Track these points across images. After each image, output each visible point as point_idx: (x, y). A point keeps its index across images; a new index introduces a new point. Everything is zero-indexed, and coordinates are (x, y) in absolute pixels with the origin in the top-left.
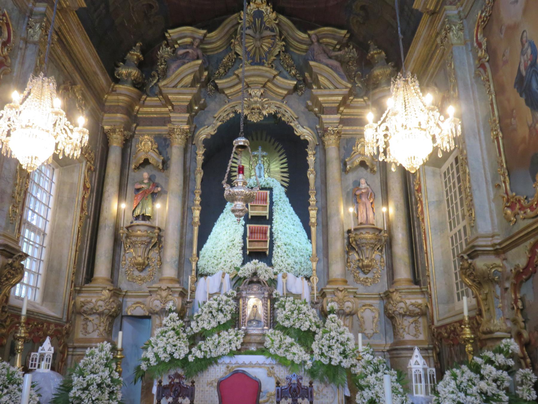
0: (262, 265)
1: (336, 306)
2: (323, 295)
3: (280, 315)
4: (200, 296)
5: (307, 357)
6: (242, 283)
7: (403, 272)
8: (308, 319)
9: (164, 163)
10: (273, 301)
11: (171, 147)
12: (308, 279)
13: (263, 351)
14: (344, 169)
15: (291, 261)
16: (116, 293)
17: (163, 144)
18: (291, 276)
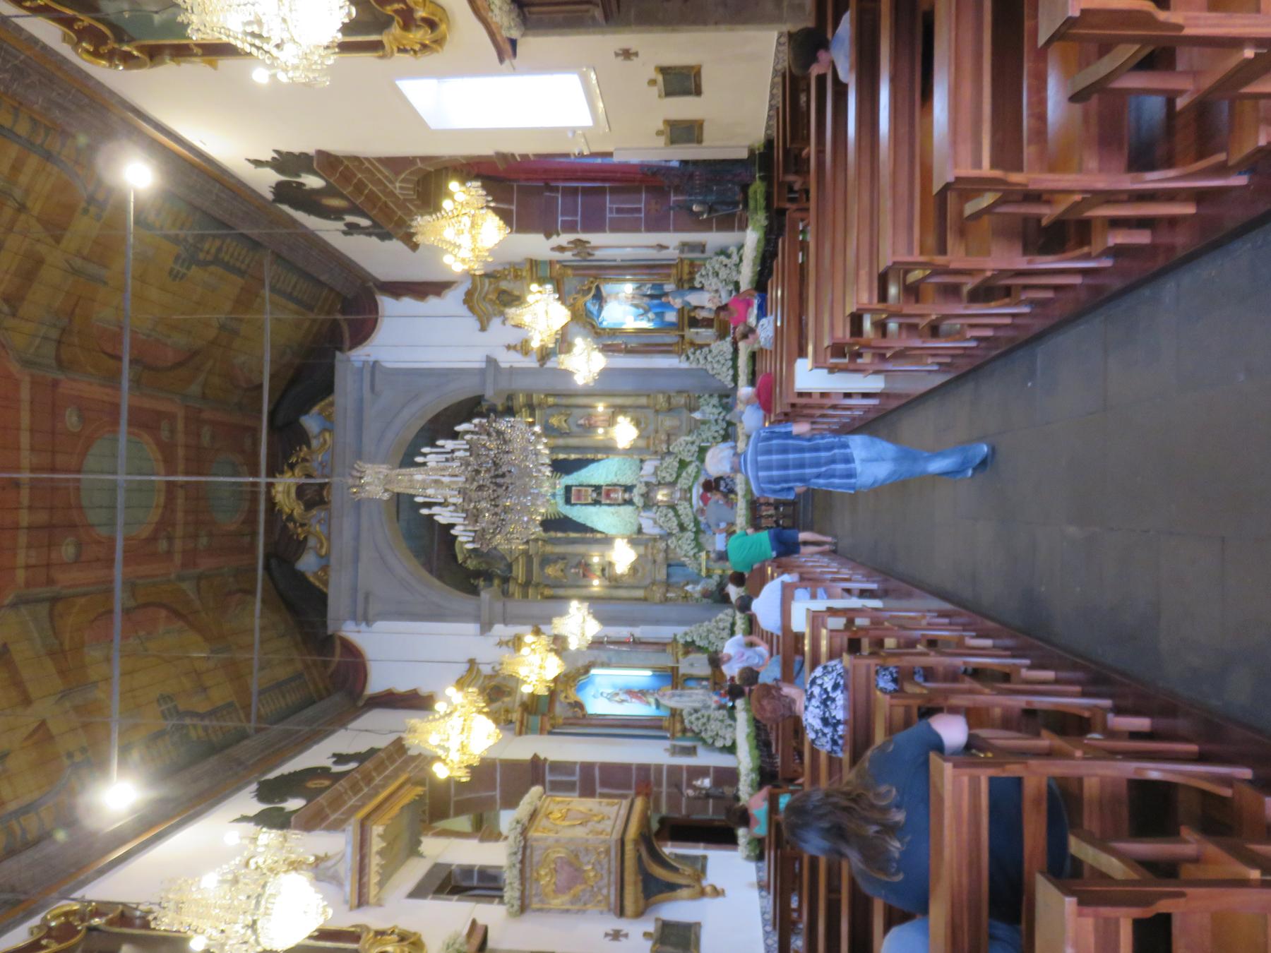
0: (635, 491)
1: (664, 448)
2: (656, 453)
3: (669, 479)
4: (656, 531)
5: (694, 465)
6: (649, 503)
7: (643, 401)
8: (672, 462)
9: (564, 559)
10: (659, 484)
11: (552, 553)
12: (642, 461)
13: (690, 489)
14: (568, 435)
15: (629, 473)
16: (653, 583)
17: (546, 561)
18: (643, 472)
